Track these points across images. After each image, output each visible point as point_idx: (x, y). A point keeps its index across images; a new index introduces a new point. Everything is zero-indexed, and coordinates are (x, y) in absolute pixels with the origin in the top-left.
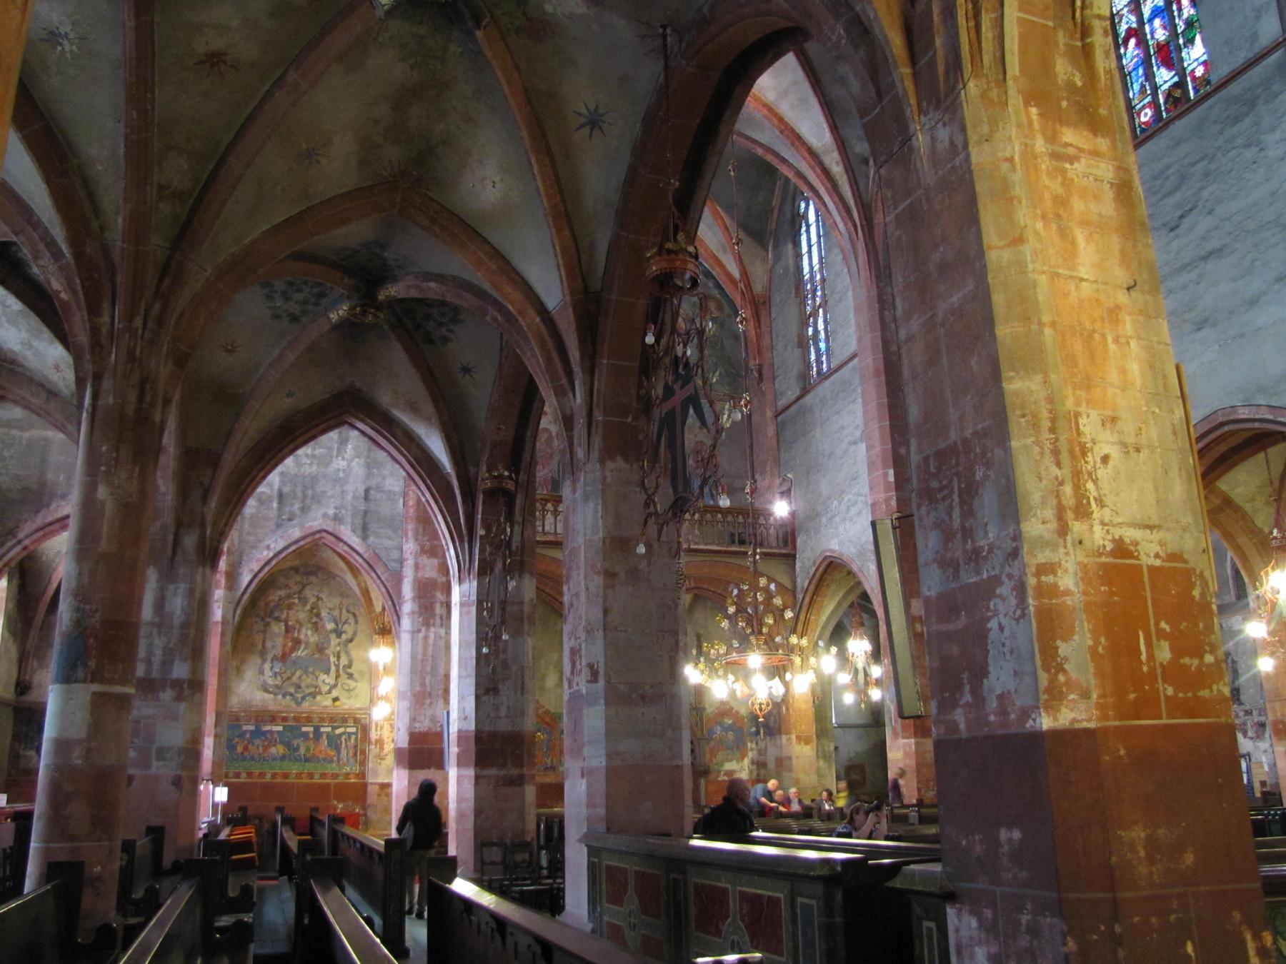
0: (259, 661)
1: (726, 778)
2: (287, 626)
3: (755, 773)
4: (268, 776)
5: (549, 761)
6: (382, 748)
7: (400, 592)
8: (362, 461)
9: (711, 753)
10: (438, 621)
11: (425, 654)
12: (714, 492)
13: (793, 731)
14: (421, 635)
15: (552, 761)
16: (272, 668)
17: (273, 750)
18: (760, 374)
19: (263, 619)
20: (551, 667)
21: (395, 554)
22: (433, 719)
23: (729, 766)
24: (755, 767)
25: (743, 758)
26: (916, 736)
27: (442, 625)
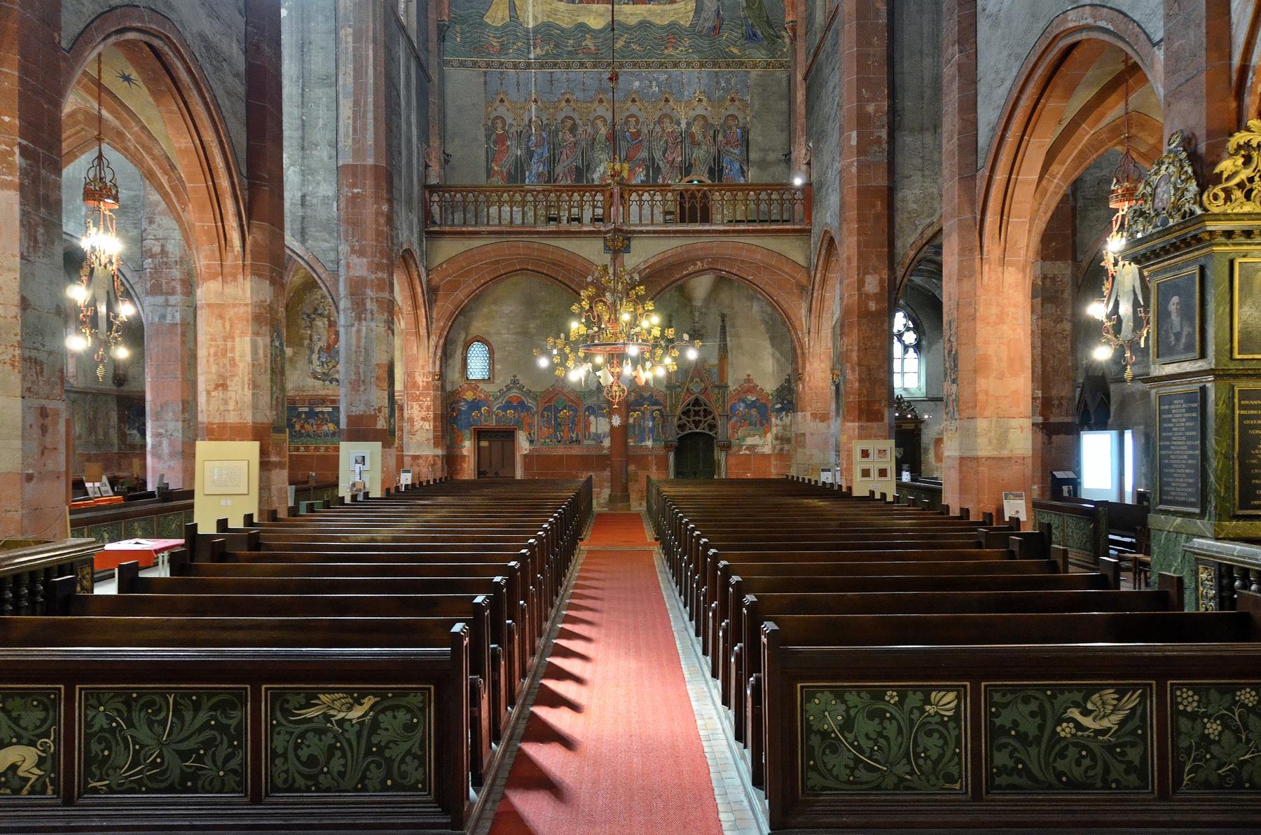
0: (308, 352)
1: (748, 452)
2: (329, 320)
3: (778, 447)
4: (322, 450)
5: (574, 436)
6: (413, 425)
7: (337, 290)
8: (297, 169)
9: (734, 427)
10: (369, 316)
11: (358, 347)
12: (745, 168)
13: (809, 408)
14: (354, 329)
15: (577, 434)
16: (319, 358)
17: (325, 428)
18: (794, 29)
19: (308, 316)
21: (332, 256)
22: (367, 404)
23: (749, 441)
24: (778, 442)
25: (766, 434)
26: (859, 419)
27: (372, 319)
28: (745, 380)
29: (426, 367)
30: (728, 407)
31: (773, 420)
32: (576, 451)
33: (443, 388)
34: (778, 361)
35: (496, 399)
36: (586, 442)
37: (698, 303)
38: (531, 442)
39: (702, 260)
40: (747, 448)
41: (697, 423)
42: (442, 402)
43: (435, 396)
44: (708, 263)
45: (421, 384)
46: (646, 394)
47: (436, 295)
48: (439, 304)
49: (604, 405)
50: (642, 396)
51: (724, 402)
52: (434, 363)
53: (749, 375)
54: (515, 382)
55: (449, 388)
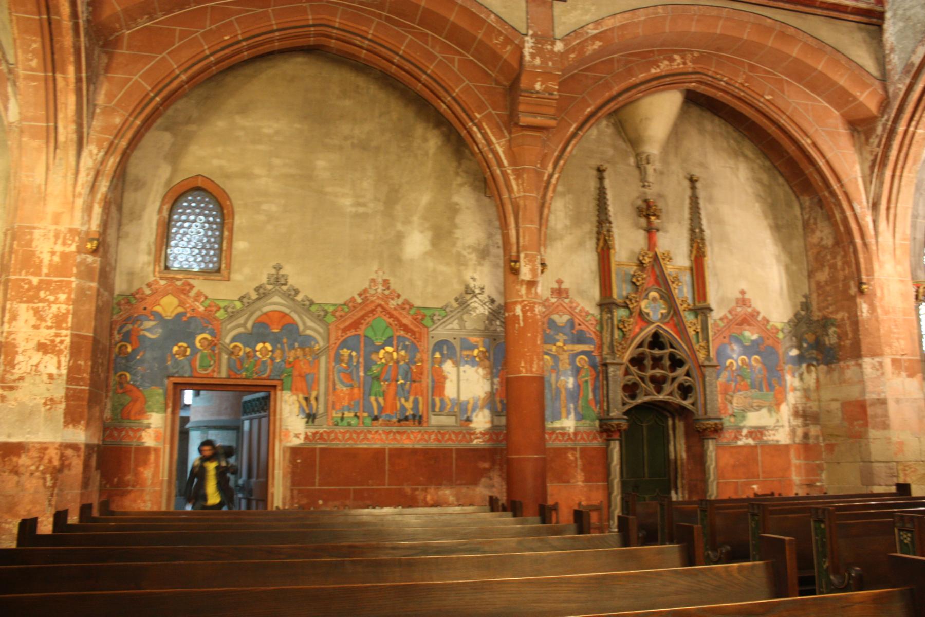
1: (751, 441)
3: (800, 432)
5: (409, 405)
15: (416, 402)
20: (416, 219)
23: (754, 419)
24: (799, 421)
25: (778, 404)
28: (738, 300)
29: (65, 219)
30: (712, 354)
31: (788, 378)
32: (411, 440)
33: (105, 276)
34: (787, 268)
35: (233, 316)
36: (434, 420)
37: (653, 149)
38: (311, 417)
39: (682, 53)
40: (750, 434)
41: (658, 383)
42: (99, 310)
43: (81, 291)
44: (694, 61)
45: (46, 258)
46: (562, 319)
47: (111, 56)
48: (119, 75)
49: (474, 340)
50: (552, 323)
51: (707, 341)
52: (88, 209)
53: (743, 292)
54: (278, 280)
55: (120, 285)
